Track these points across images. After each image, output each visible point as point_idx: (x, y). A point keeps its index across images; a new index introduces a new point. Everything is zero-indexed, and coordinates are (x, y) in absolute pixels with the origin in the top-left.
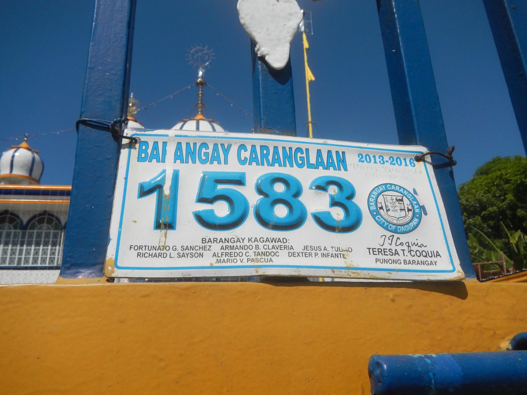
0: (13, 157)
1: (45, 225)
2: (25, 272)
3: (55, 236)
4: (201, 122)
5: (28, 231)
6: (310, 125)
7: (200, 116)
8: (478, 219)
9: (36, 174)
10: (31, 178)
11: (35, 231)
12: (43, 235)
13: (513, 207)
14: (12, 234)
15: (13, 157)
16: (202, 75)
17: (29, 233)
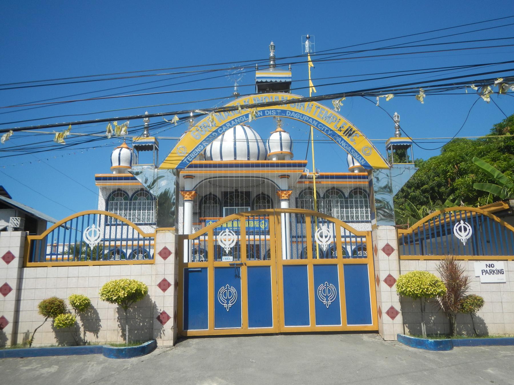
0: (120, 154)
5: (132, 202)
8: (418, 192)
11: (137, 201)
13: (439, 185)
15: (120, 154)
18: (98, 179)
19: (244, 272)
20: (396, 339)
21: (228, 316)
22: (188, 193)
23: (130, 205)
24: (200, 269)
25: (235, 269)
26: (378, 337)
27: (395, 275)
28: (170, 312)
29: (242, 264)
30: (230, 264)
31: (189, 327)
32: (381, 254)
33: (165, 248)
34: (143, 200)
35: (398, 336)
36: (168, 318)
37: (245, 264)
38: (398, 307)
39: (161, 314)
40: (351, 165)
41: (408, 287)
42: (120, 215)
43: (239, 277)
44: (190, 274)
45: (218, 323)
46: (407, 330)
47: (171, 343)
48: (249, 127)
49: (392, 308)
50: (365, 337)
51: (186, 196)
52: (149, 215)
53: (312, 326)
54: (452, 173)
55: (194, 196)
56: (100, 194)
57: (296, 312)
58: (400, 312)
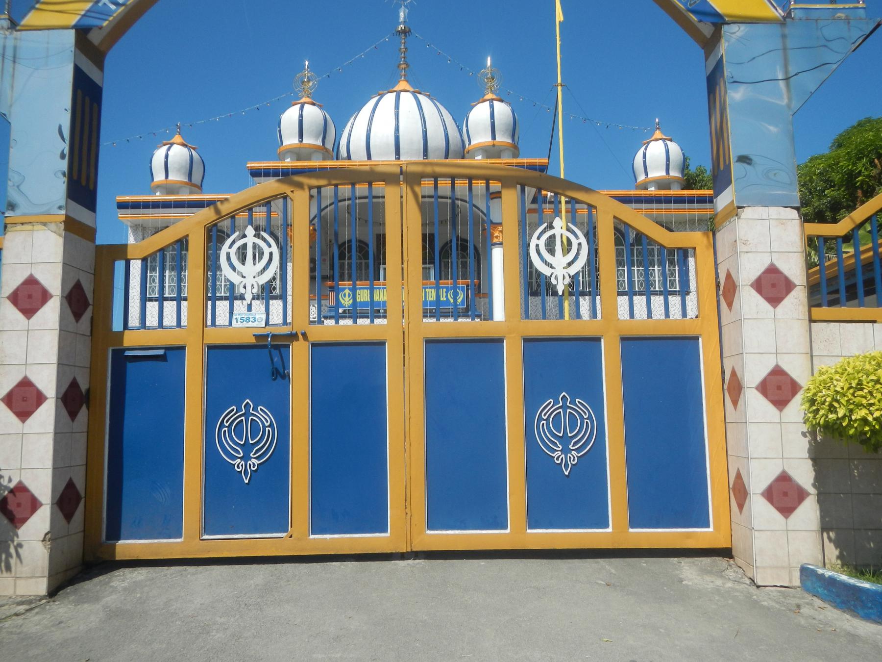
0: (167, 157)
4: (402, 94)
6: (559, 88)
7: (403, 85)
9: (196, 178)
10: (192, 185)
15: (167, 157)
18: (122, 206)
19: (299, 360)
20: (797, 582)
21: (246, 498)
24: (161, 352)
25: (271, 349)
26: (730, 573)
27: (797, 369)
28: (42, 487)
29: (293, 337)
30: (257, 337)
31: (124, 531)
32: (750, 301)
33: (31, 281)
35: (805, 571)
36: (35, 505)
37: (304, 335)
38: (804, 475)
39: (12, 491)
40: (641, 178)
41: (859, 405)
43: (285, 377)
44: (130, 365)
45: (213, 521)
46: (832, 552)
47: (41, 587)
48: (429, 96)
49: (784, 478)
50: (687, 569)
53: (515, 531)
54: (868, 176)
57: (463, 486)
58: (812, 491)
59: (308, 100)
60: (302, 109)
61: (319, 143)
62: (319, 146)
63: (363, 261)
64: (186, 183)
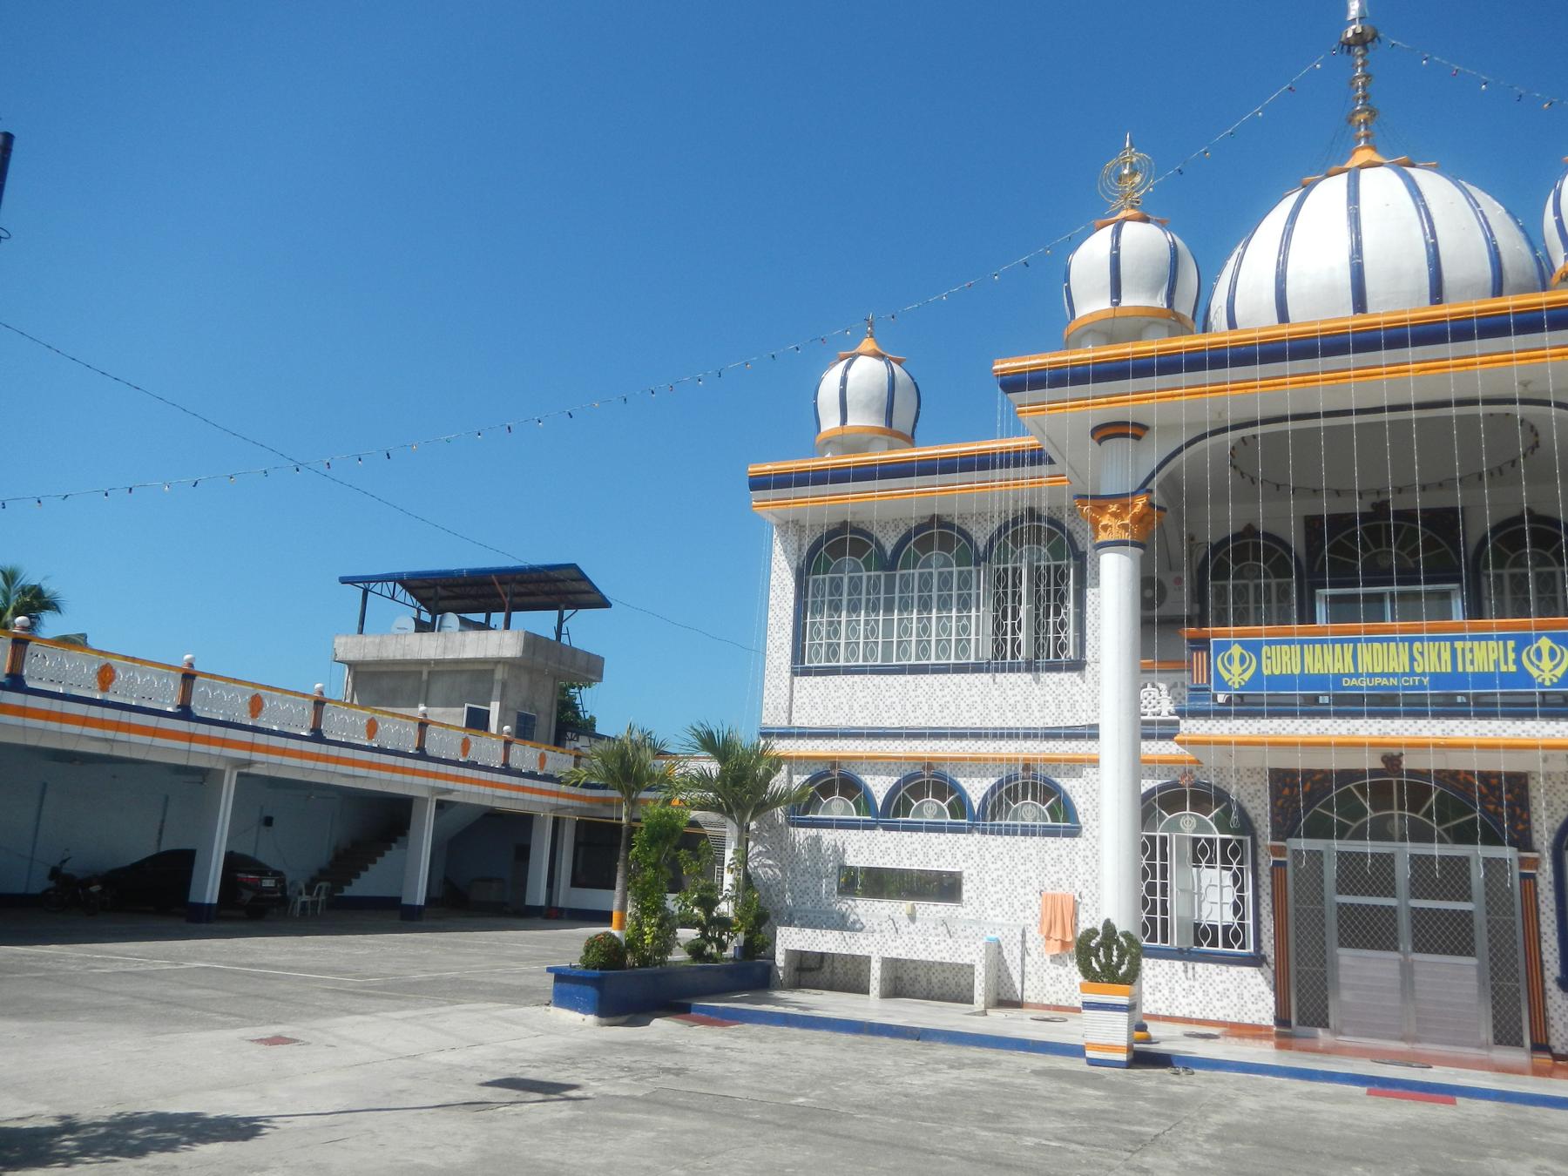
0: (844, 381)
1: (935, 554)
2: (902, 678)
3: (965, 582)
4: (1364, 173)
5: (898, 573)
7: (1364, 155)
9: (903, 420)
10: (890, 431)
11: (917, 572)
12: (935, 581)
14: (846, 580)
15: (844, 381)
16: (1361, 9)
17: (902, 576)
22: (1113, 508)
23: (890, 589)
34: (936, 564)
42: (854, 629)
48: (1437, 169)
51: (1105, 520)
52: (965, 629)
55: (1139, 519)
56: (778, 548)
59: (1131, 212)
60: (1117, 233)
61: (1160, 302)
62: (1156, 312)
63: (1273, 582)
64: (881, 431)
